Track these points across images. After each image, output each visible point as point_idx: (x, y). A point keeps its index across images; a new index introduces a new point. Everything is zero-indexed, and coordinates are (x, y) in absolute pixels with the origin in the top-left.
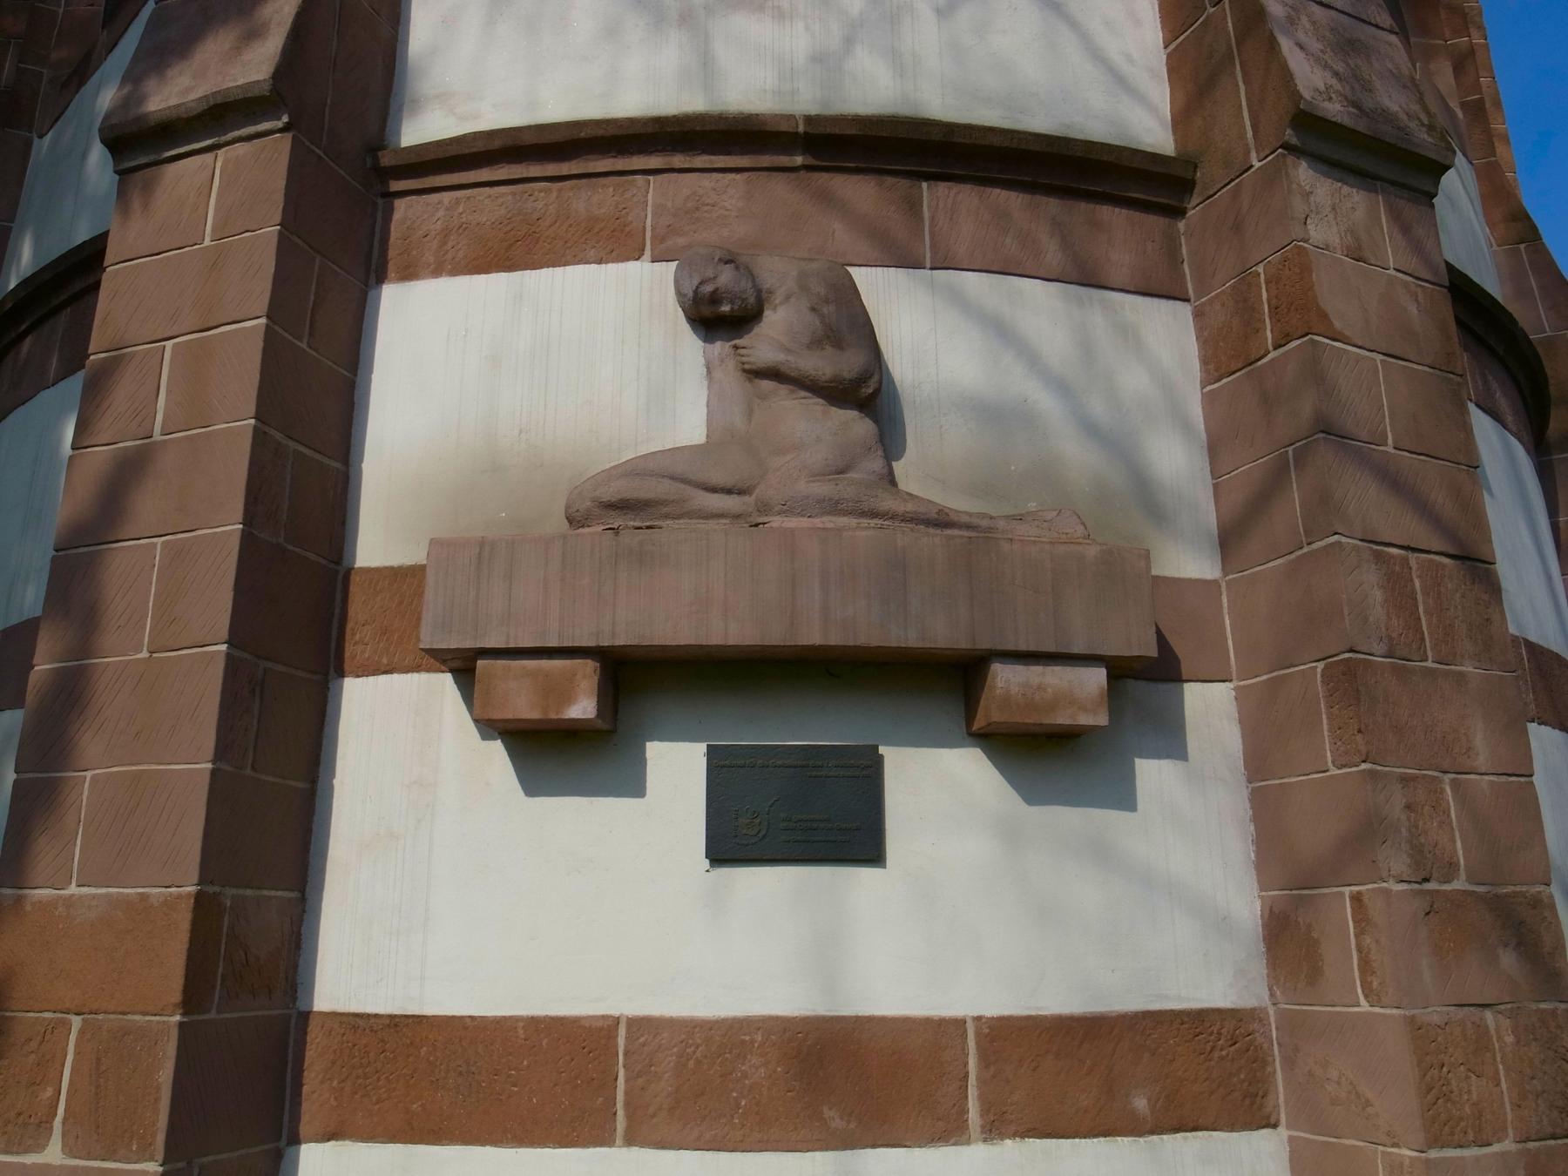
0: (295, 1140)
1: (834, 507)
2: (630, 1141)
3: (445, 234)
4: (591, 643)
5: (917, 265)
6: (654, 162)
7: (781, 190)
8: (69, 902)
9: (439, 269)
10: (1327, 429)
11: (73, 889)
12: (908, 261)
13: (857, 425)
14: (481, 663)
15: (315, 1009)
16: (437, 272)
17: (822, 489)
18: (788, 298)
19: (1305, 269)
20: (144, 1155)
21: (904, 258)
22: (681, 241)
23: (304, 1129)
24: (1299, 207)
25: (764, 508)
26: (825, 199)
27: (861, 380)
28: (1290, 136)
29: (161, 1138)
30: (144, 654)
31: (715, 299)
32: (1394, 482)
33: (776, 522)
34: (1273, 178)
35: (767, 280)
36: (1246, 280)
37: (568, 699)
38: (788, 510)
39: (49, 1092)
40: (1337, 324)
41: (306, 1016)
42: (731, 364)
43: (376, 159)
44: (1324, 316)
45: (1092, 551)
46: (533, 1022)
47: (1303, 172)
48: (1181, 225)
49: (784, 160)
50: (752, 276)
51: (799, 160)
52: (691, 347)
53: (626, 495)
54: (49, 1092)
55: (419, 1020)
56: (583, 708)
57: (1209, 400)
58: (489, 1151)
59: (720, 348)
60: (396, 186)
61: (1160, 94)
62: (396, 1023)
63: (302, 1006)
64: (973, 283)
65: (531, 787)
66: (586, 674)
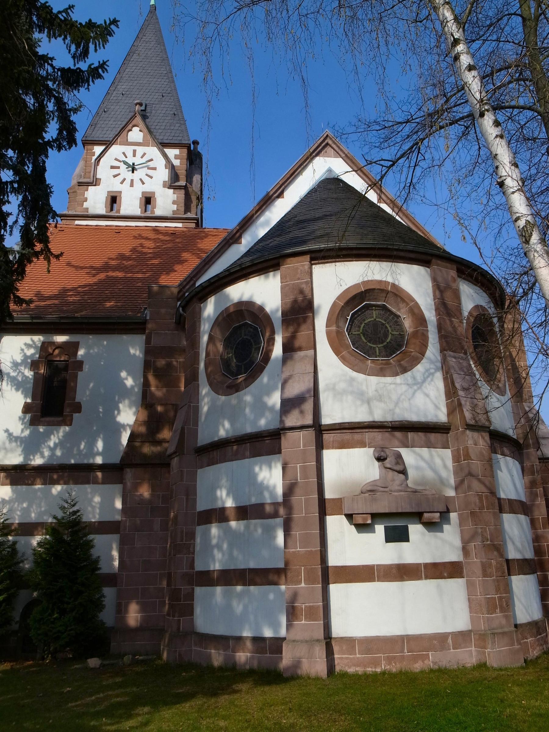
0: (329, 584)
1: (401, 491)
2: (378, 581)
3: (333, 441)
4: (370, 512)
5: (408, 447)
6: (367, 430)
7: (387, 434)
8: (298, 551)
9: (333, 448)
10: (470, 474)
11: (298, 549)
12: (407, 447)
13: (402, 476)
14: (354, 515)
15: (330, 565)
16: (333, 448)
17: (400, 488)
18: (391, 457)
19: (468, 450)
20: (319, 583)
21: (406, 446)
22: (373, 444)
23: (330, 583)
24: (467, 438)
25: (391, 491)
26: (394, 436)
27: (404, 470)
28: (465, 427)
29: (321, 582)
30: (304, 515)
31: (381, 457)
32: (480, 480)
33: (393, 493)
34: (463, 433)
35: (388, 453)
36: (458, 450)
37: (367, 520)
38: (394, 492)
39: (300, 577)
40: (472, 458)
41: (328, 567)
42: (382, 466)
43: (320, 428)
44: (470, 457)
45: (437, 496)
46: (363, 566)
47: (468, 432)
48: (449, 435)
49: (387, 430)
50: (386, 453)
51: (390, 430)
52: (376, 463)
53: (371, 489)
54: (300, 577)
55: (346, 566)
56: (369, 522)
57: (453, 466)
58: (358, 583)
59: (380, 463)
60: (323, 432)
61: (444, 410)
62: (342, 567)
63: (327, 565)
64: (417, 450)
65: (359, 533)
66: (369, 516)
